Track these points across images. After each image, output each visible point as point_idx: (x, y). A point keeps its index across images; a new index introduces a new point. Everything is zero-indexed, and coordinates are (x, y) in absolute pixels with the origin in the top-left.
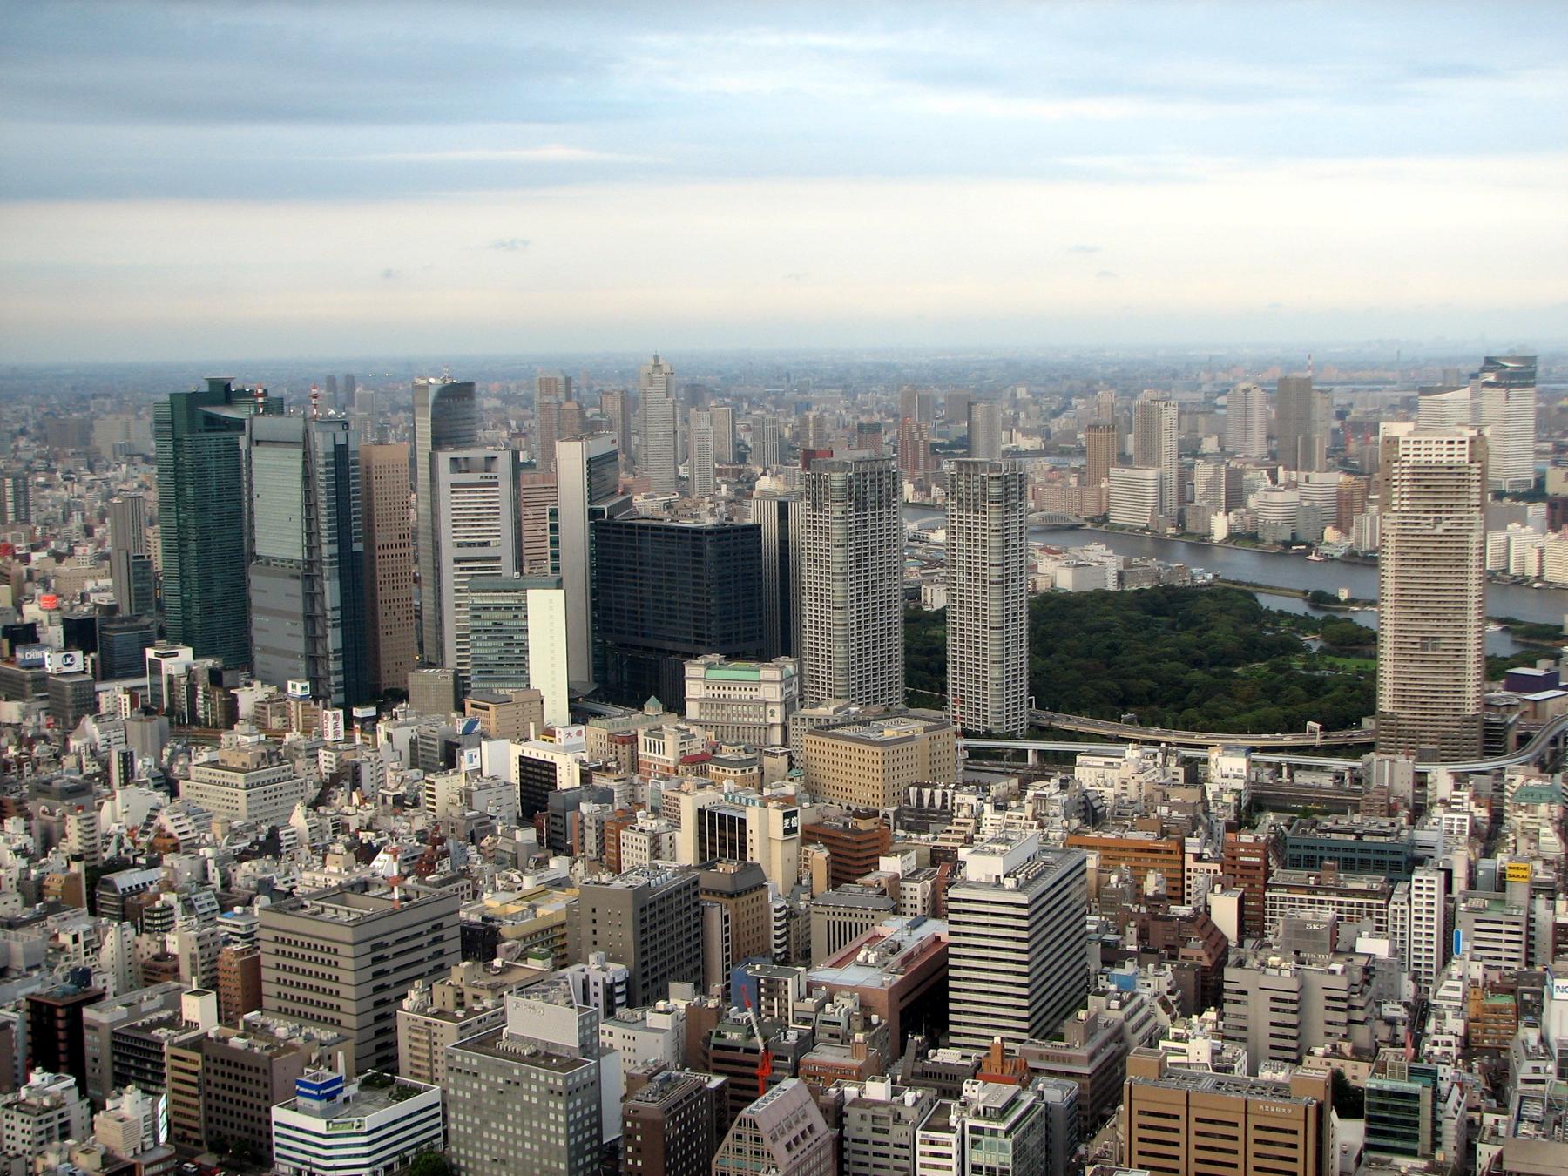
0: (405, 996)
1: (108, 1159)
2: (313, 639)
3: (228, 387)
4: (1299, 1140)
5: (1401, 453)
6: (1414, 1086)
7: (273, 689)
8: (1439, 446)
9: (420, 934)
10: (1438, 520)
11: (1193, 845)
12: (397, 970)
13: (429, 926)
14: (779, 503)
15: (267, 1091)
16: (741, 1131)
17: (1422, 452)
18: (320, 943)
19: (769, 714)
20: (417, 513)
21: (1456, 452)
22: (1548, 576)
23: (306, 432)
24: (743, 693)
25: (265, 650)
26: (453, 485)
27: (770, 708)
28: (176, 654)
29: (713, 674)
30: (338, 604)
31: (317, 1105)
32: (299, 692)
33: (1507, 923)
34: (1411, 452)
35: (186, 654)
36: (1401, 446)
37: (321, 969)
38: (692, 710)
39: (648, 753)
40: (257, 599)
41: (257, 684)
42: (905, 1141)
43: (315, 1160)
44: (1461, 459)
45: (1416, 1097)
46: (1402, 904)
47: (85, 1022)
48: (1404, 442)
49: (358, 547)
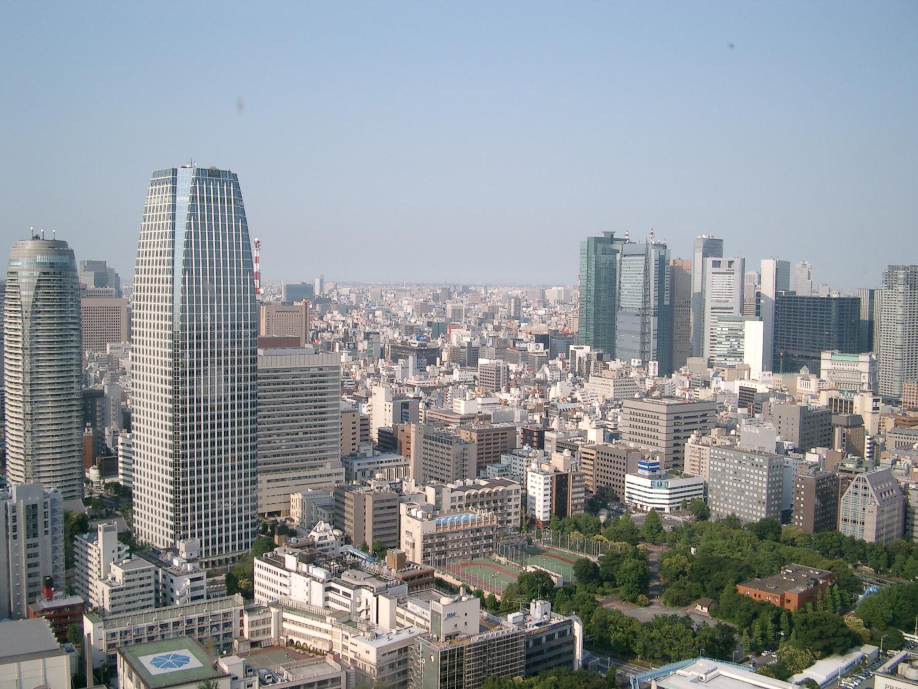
0: (689, 437)
1: (556, 471)
2: (643, 343)
3: (612, 236)
7: (625, 363)
9: (696, 417)
12: (685, 417)
13: (701, 413)
14: (870, 291)
15: (625, 467)
16: (858, 483)
18: (651, 414)
19: (862, 378)
20: (696, 288)
23: (647, 249)
24: (850, 367)
25: (621, 349)
26: (713, 273)
27: (863, 375)
28: (583, 348)
29: (834, 357)
30: (656, 328)
31: (647, 473)
32: (636, 364)
35: (587, 349)
37: (650, 426)
38: (824, 375)
39: (802, 388)
40: (619, 326)
41: (618, 360)
43: (645, 499)
47: (546, 438)
49: (667, 303)
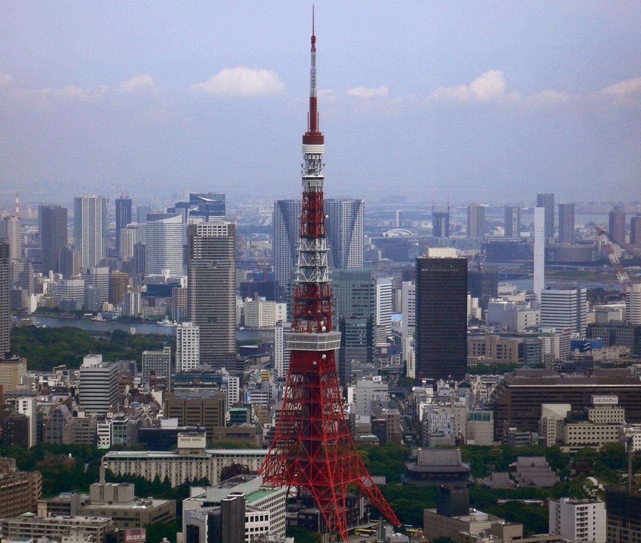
4: (218, 410)
5: (198, 232)
6: (245, 409)
8: (215, 229)
10: (215, 263)
11: (138, 381)
17: (207, 232)
21: (222, 232)
22: (246, 323)
33: (263, 393)
34: (202, 232)
36: (198, 229)
42: (94, 428)
44: (224, 234)
45: (245, 412)
46: (225, 389)
48: (199, 227)
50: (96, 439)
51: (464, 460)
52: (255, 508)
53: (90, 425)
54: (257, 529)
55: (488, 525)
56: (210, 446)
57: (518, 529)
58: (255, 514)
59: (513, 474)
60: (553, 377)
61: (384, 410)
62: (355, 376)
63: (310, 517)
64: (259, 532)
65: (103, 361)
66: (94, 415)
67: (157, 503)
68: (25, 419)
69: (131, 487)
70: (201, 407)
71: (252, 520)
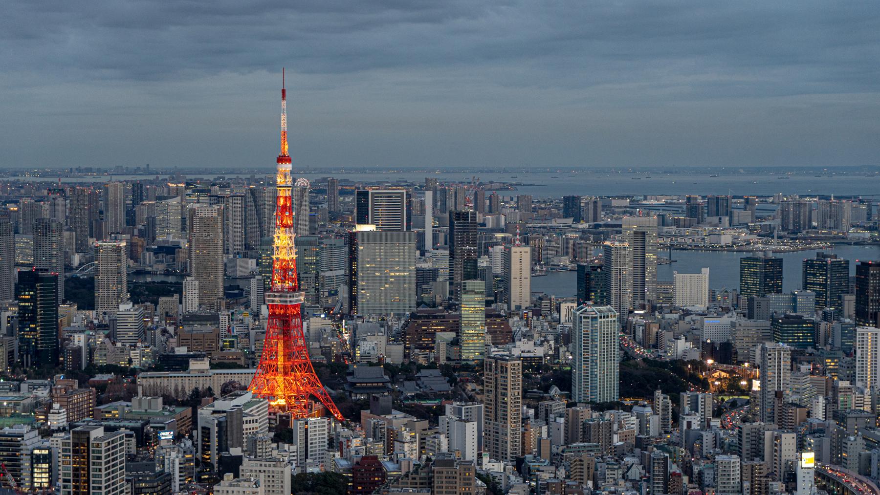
10: (208, 235)
50: (130, 361)
51: (385, 375)
52: (248, 415)
53: (125, 351)
54: (250, 429)
55: (406, 421)
56: (213, 366)
57: (425, 424)
58: (248, 418)
59: (419, 382)
60: (443, 314)
61: (329, 338)
62: (308, 313)
63: (284, 418)
64: (252, 431)
65: (133, 306)
66: (127, 345)
67: (179, 410)
68: (80, 348)
69: (160, 400)
70: (202, 338)
71: (247, 423)
